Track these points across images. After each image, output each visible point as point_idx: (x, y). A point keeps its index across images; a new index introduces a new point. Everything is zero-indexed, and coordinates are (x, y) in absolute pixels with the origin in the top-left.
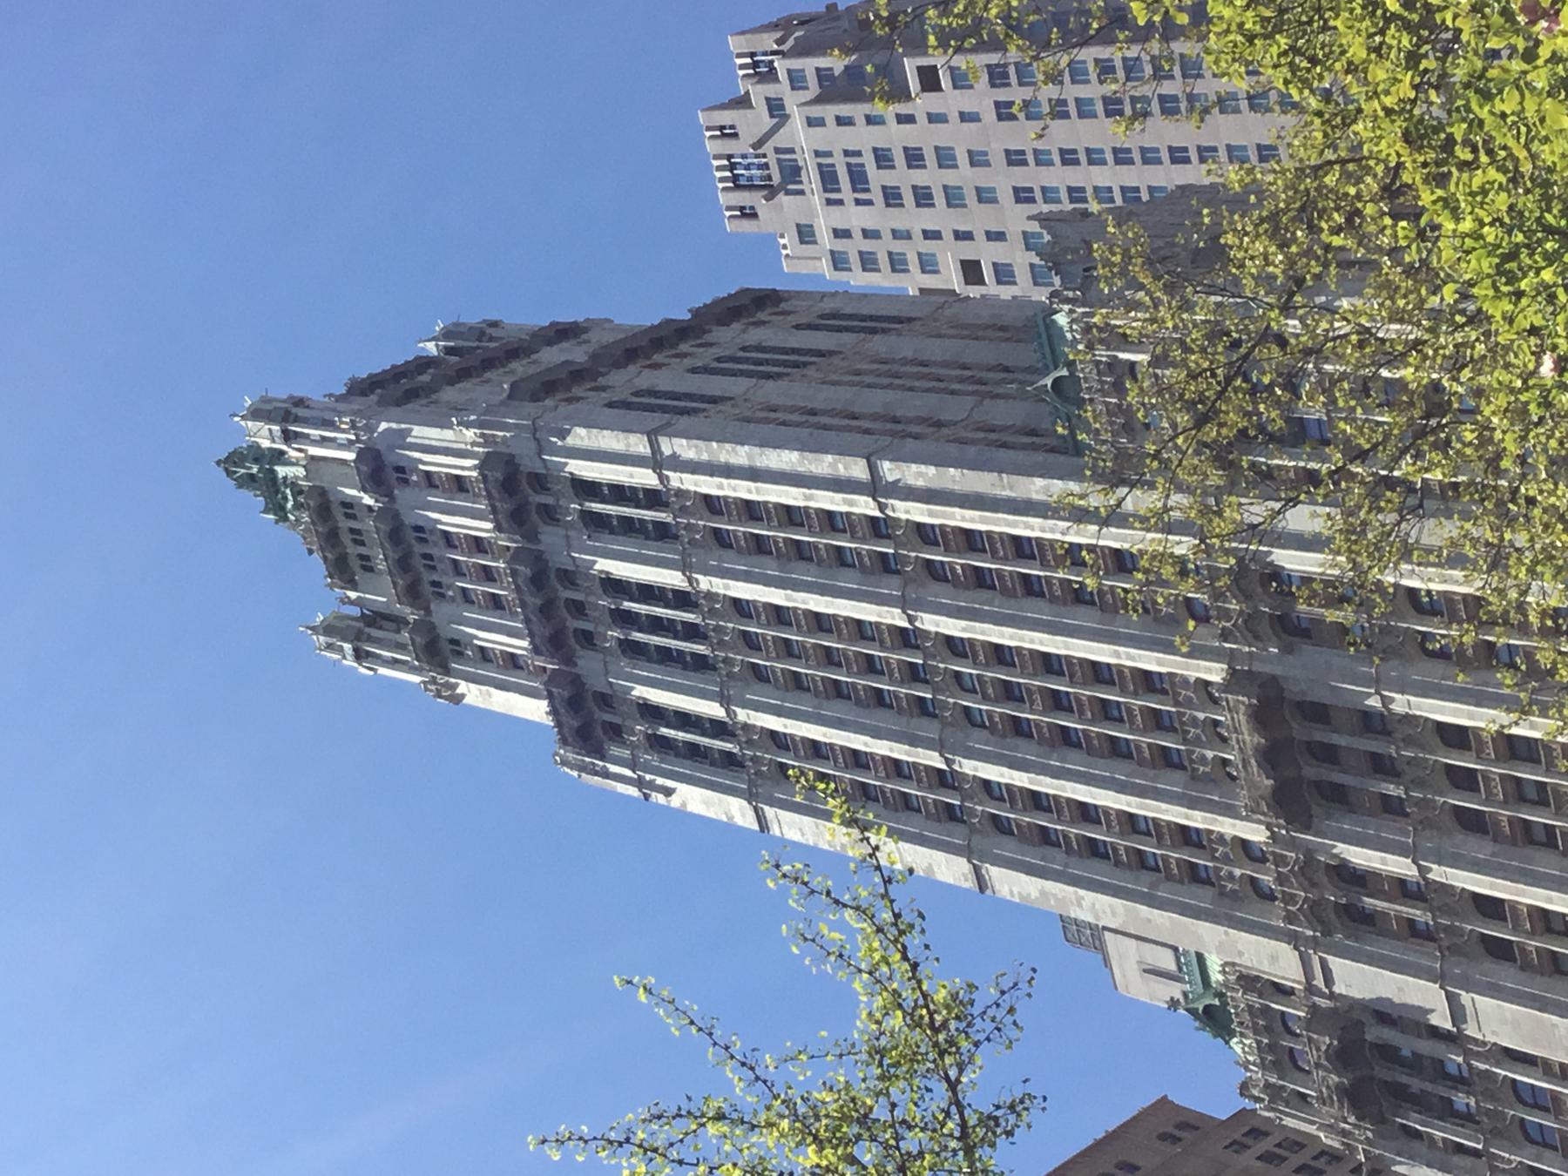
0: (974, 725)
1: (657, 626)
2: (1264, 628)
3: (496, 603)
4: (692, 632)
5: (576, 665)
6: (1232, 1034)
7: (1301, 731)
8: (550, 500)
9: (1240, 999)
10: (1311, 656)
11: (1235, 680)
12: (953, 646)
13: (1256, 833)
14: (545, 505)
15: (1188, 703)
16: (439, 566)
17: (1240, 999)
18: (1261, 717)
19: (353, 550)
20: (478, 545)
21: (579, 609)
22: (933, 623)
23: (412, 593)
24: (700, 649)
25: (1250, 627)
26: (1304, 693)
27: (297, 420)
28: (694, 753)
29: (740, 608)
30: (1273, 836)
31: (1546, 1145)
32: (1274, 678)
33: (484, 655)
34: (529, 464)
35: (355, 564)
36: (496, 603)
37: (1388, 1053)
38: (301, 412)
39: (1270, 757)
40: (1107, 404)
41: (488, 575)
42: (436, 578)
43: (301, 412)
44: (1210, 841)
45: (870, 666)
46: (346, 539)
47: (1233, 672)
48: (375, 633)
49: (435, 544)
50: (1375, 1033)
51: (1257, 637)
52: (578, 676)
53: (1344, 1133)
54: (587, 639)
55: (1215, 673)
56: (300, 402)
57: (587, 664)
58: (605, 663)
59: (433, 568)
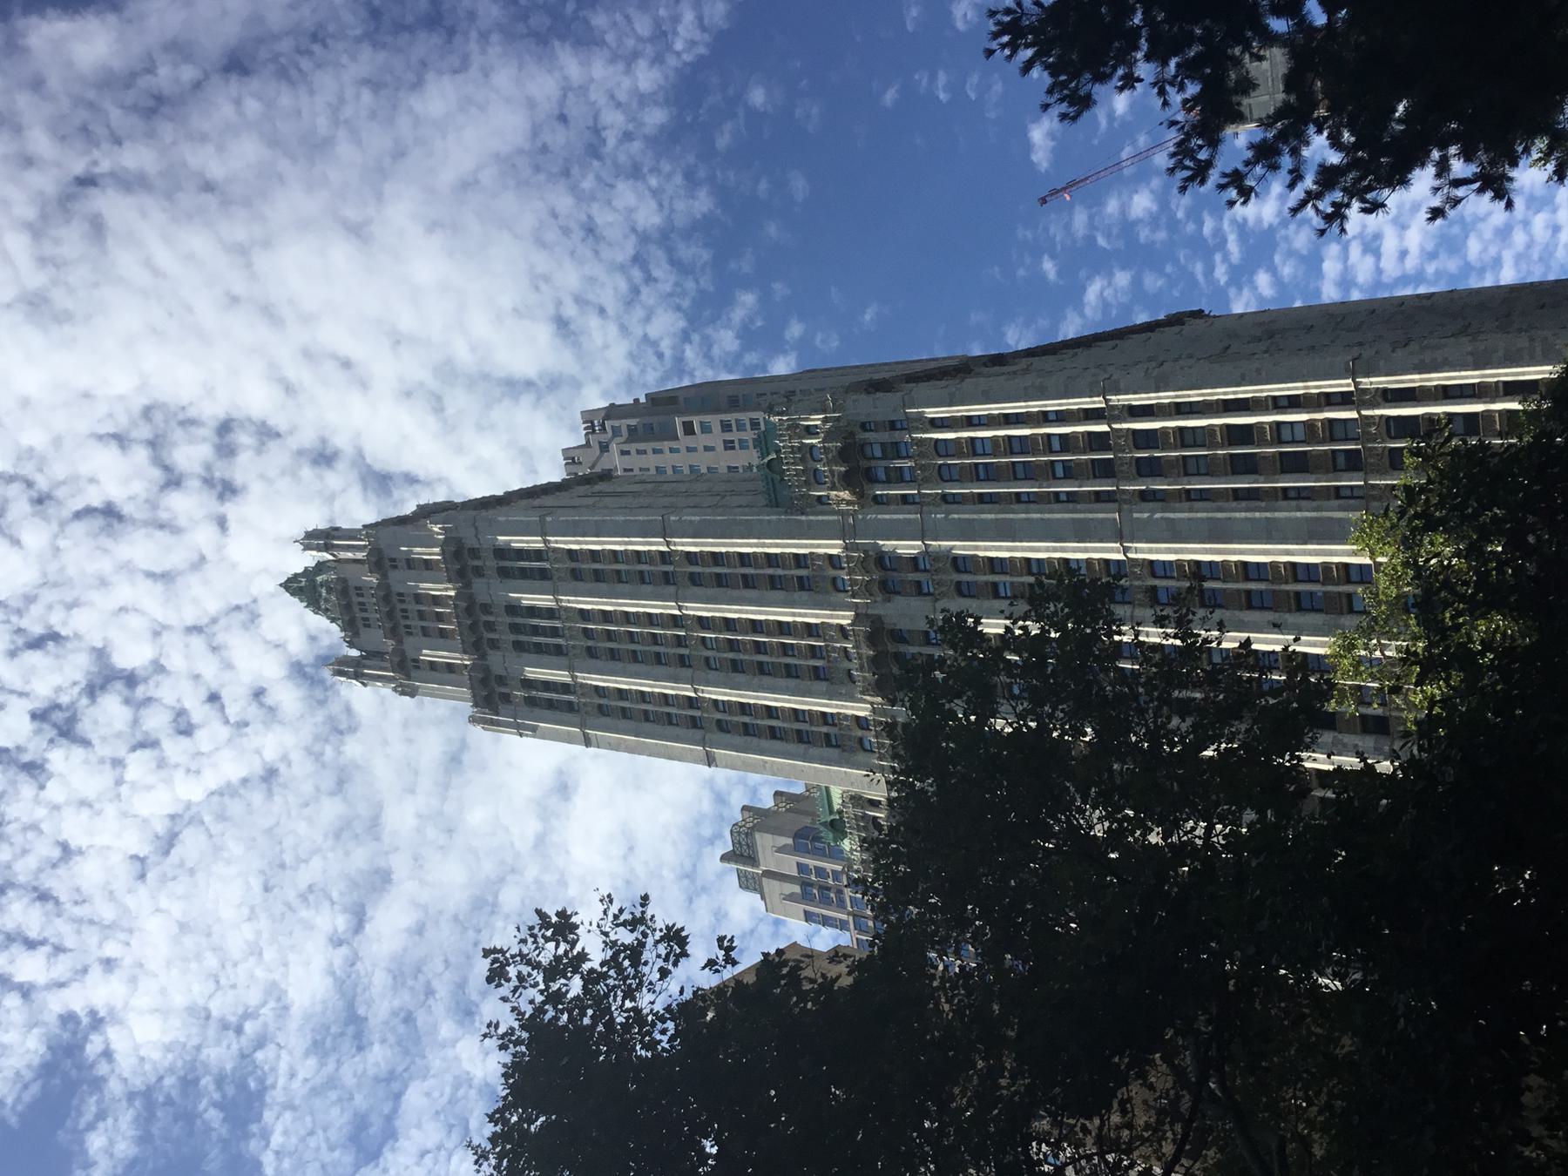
0: (711, 669)
2: (876, 589)
4: (554, 632)
5: (486, 660)
7: (892, 648)
11: (857, 619)
12: (703, 623)
13: (861, 710)
14: (477, 567)
15: (832, 639)
18: (872, 639)
19: (359, 615)
21: (490, 626)
23: (393, 633)
24: (560, 641)
25: (867, 589)
26: (895, 624)
28: (551, 705)
29: (584, 615)
30: (874, 711)
32: (879, 617)
34: (470, 542)
36: (443, 634)
38: (335, 533)
39: (876, 663)
40: (796, 470)
41: (440, 617)
42: (408, 623)
43: (335, 533)
44: (839, 719)
46: (356, 609)
47: (857, 615)
49: (409, 603)
51: (871, 595)
52: (488, 666)
54: (494, 644)
55: (844, 618)
57: (495, 660)
58: (504, 656)
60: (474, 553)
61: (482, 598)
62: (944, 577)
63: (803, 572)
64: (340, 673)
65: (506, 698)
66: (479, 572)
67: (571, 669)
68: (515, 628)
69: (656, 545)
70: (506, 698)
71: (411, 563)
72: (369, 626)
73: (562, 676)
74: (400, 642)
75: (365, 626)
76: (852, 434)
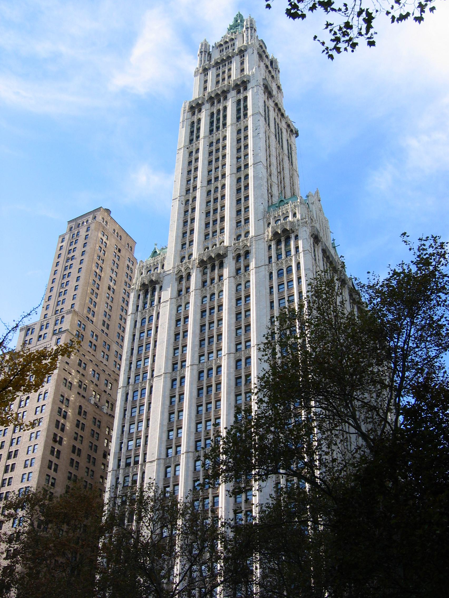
1: (218, 120)
3: (218, 82)
6: (152, 257)
7: (217, 263)
8: (242, 92)
9: (160, 258)
10: (233, 262)
16: (224, 68)
17: (160, 258)
20: (229, 77)
21: (219, 102)
22: (228, 181)
23: (217, 64)
27: (251, 30)
28: (192, 132)
31: (142, 323)
33: (206, 82)
34: (249, 86)
35: (221, 48)
37: (154, 290)
38: (253, 31)
41: (224, 79)
42: (221, 68)
43: (253, 31)
45: (217, 168)
46: (227, 45)
47: (227, 247)
48: (207, 55)
50: (158, 287)
53: (136, 283)
55: (226, 243)
56: (255, 30)
59: (223, 67)
60: (245, 89)
61: (229, 96)
62: (243, 279)
63: (243, 223)
64: (202, 46)
65: (193, 114)
66: (239, 92)
67: (204, 137)
68: (219, 111)
69: (251, 161)
70: (193, 114)
71: (242, 63)
72: (220, 52)
73: (202, 134)
74: (214, 67)
75: (221, 51)
76: (293, 232)
